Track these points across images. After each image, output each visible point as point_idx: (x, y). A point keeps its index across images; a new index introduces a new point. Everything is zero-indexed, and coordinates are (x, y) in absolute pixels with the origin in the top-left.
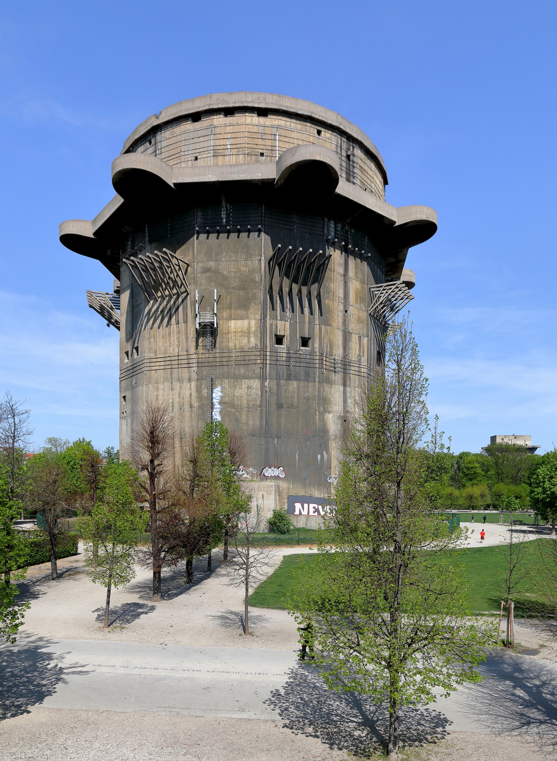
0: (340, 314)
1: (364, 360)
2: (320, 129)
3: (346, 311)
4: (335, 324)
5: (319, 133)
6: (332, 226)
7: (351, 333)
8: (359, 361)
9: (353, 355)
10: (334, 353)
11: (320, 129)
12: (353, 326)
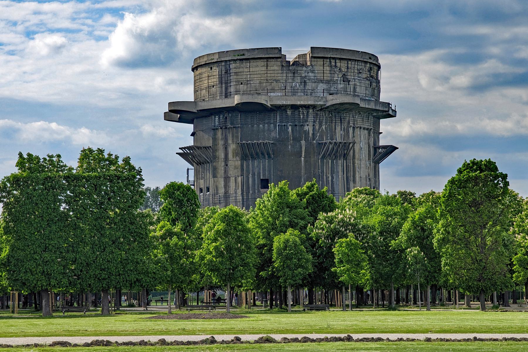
0: (223, 168)
1: (239, 191)
2: (211, 66)
3: (227, 165)
4: (219, 176)
5: (211, 68)
6: (217, 119)
7: (230, 177)
8: (236, 193)
9: (232, 191)
10: (219, 192)
11: (211, 66)
12: (232, 172)
